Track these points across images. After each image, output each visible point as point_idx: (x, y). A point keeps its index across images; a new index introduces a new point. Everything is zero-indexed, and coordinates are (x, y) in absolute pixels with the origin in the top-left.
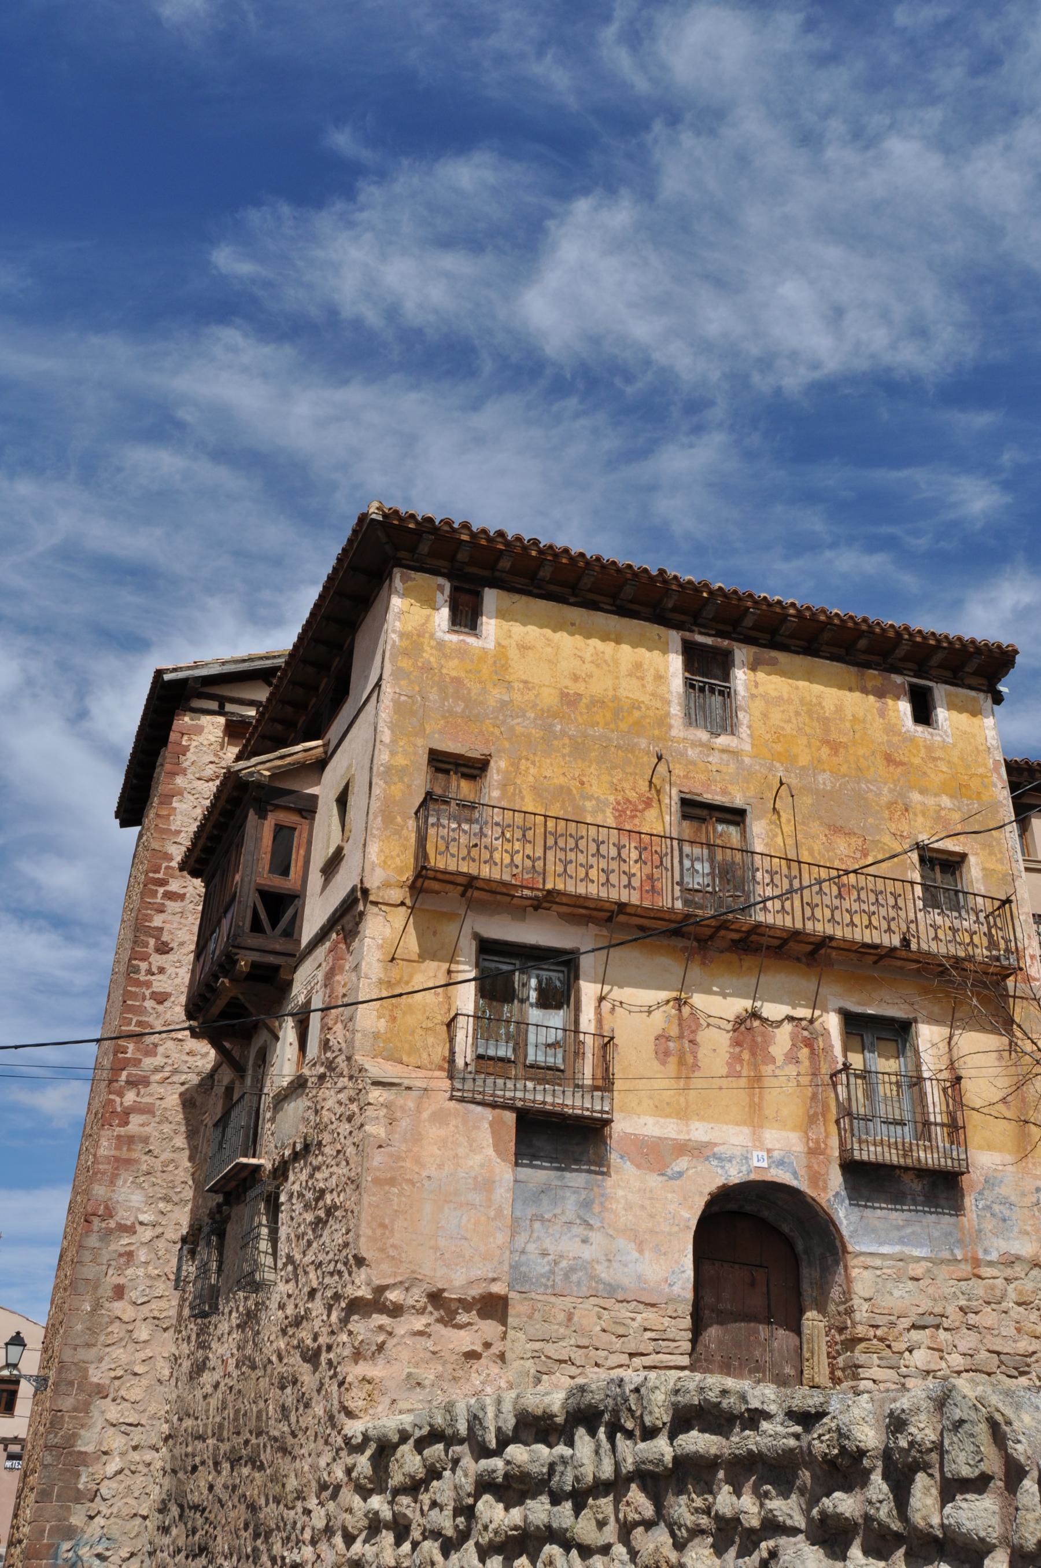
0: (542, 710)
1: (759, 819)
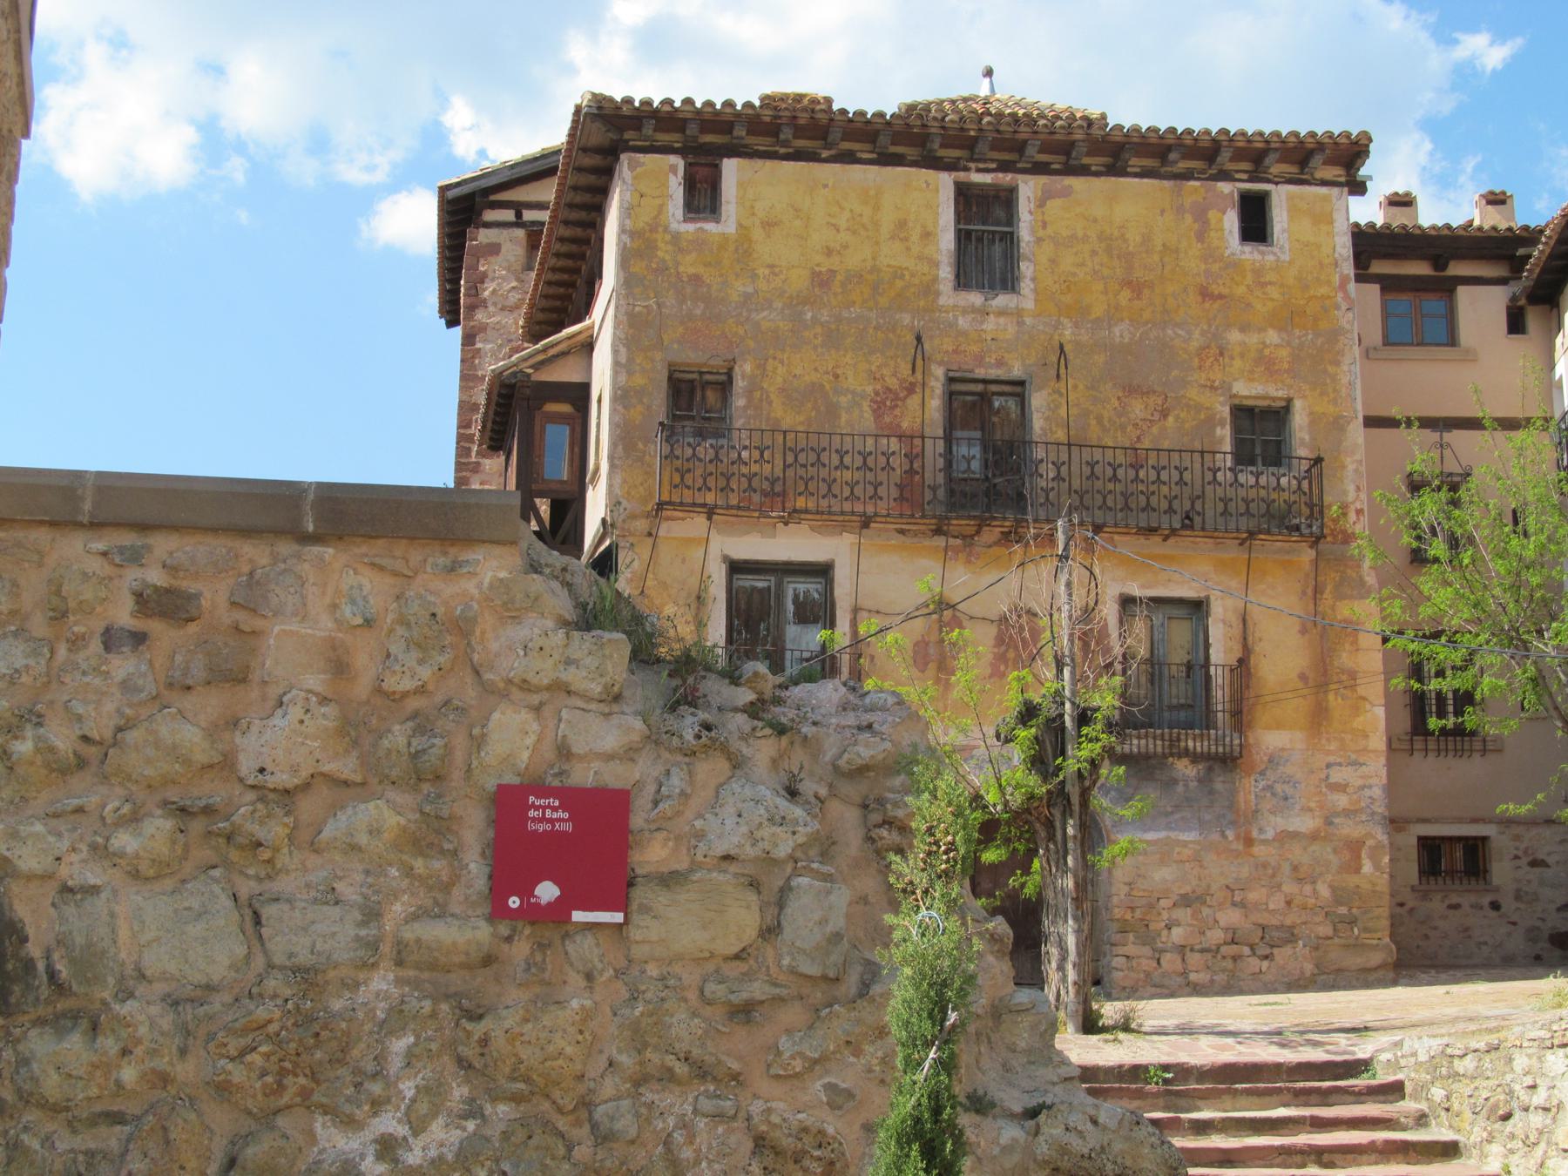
0: (791, 297)
1: (1040, 388)
